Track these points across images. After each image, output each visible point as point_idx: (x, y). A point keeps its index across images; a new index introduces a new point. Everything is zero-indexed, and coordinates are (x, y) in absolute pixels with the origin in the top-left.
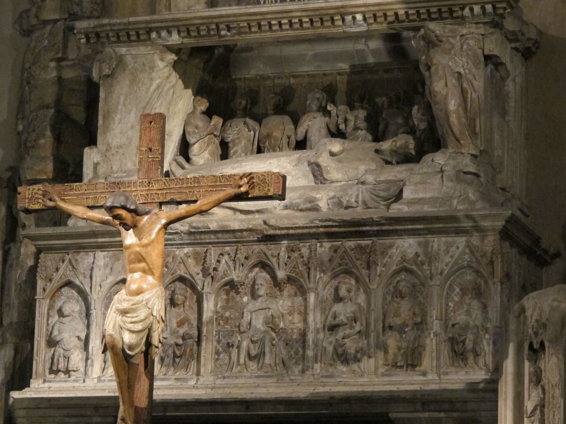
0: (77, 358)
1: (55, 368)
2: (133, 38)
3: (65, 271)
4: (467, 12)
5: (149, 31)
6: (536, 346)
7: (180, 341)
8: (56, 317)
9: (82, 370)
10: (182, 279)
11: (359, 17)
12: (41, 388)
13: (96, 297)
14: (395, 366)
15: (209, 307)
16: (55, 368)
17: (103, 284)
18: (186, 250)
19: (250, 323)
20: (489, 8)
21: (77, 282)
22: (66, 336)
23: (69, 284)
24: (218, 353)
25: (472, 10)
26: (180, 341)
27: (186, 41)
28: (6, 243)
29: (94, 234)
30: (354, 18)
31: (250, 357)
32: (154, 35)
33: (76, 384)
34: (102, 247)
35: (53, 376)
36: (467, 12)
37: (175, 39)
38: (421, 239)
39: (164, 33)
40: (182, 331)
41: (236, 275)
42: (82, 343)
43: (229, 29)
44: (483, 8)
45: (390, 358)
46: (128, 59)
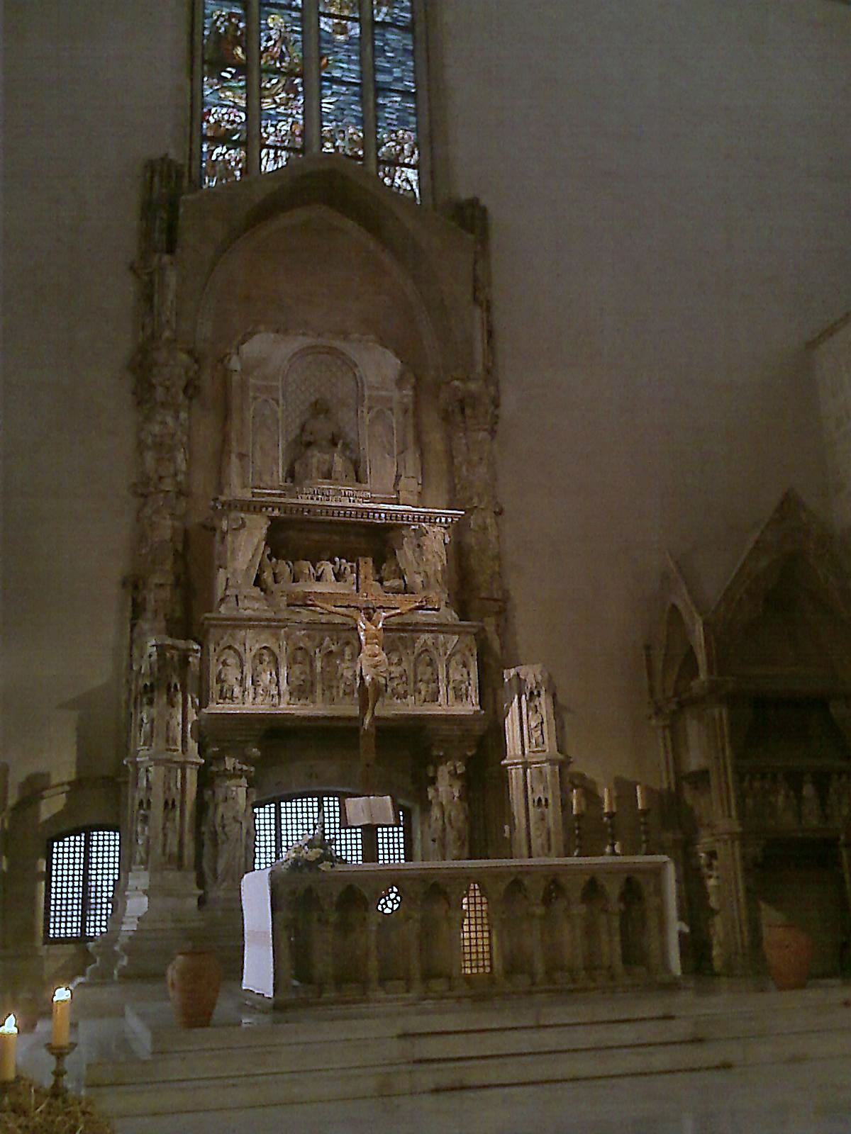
0: (237, 690)
1: (224, 696)
2: (252, 509)
3: (227, 640)
4: (438, 520)
5: (261, 507)
6: (536, 693)
7: (302, 683)
8: (221, 667)
9: (240, 697)
10: (301, 648)
11: (383, 515)
12: (216, 708)
13: (248, 657)
14: (425, 701)
15: (318, 665)
16: (224, 696)
17: (252, 648)
18: (303, 632)
19: (342, 675)
20: (450, 520)
21: (236, 647)
22: (230, 677)
23: (230, 647)
24: (324, 690)
25: (441, 520)
26: (302, 683)
27: (282, 515)
28: (132, 619)
29: (250, 619)
30: (380, 516)
31: (345, 693)
32: (264, 510)
33: (238, 706)
34: (250, 627)
35: (221, 701)
36: (438, 520)
37: (276, 513)
38: (432, 635)
39: (270, 509)
40: (303, 677)
41: (333, 648)
42: (239, 682)
43: (309, 512)
44: (446, 520)
45: (422, 697)
46: (246, 520)
